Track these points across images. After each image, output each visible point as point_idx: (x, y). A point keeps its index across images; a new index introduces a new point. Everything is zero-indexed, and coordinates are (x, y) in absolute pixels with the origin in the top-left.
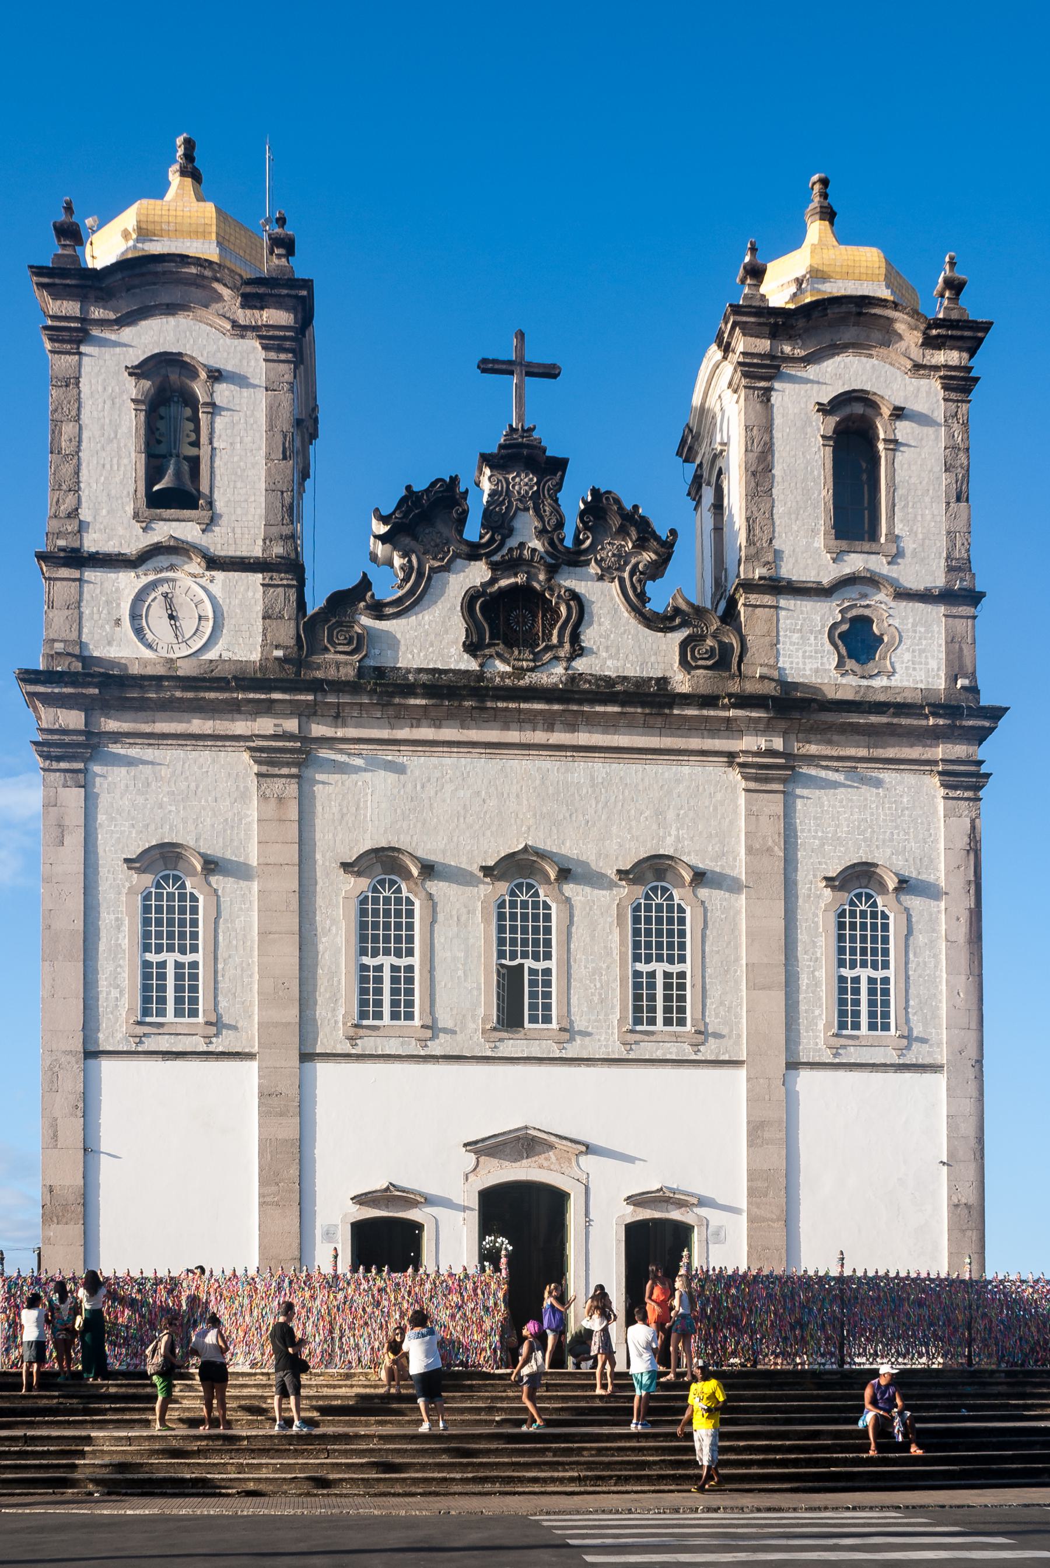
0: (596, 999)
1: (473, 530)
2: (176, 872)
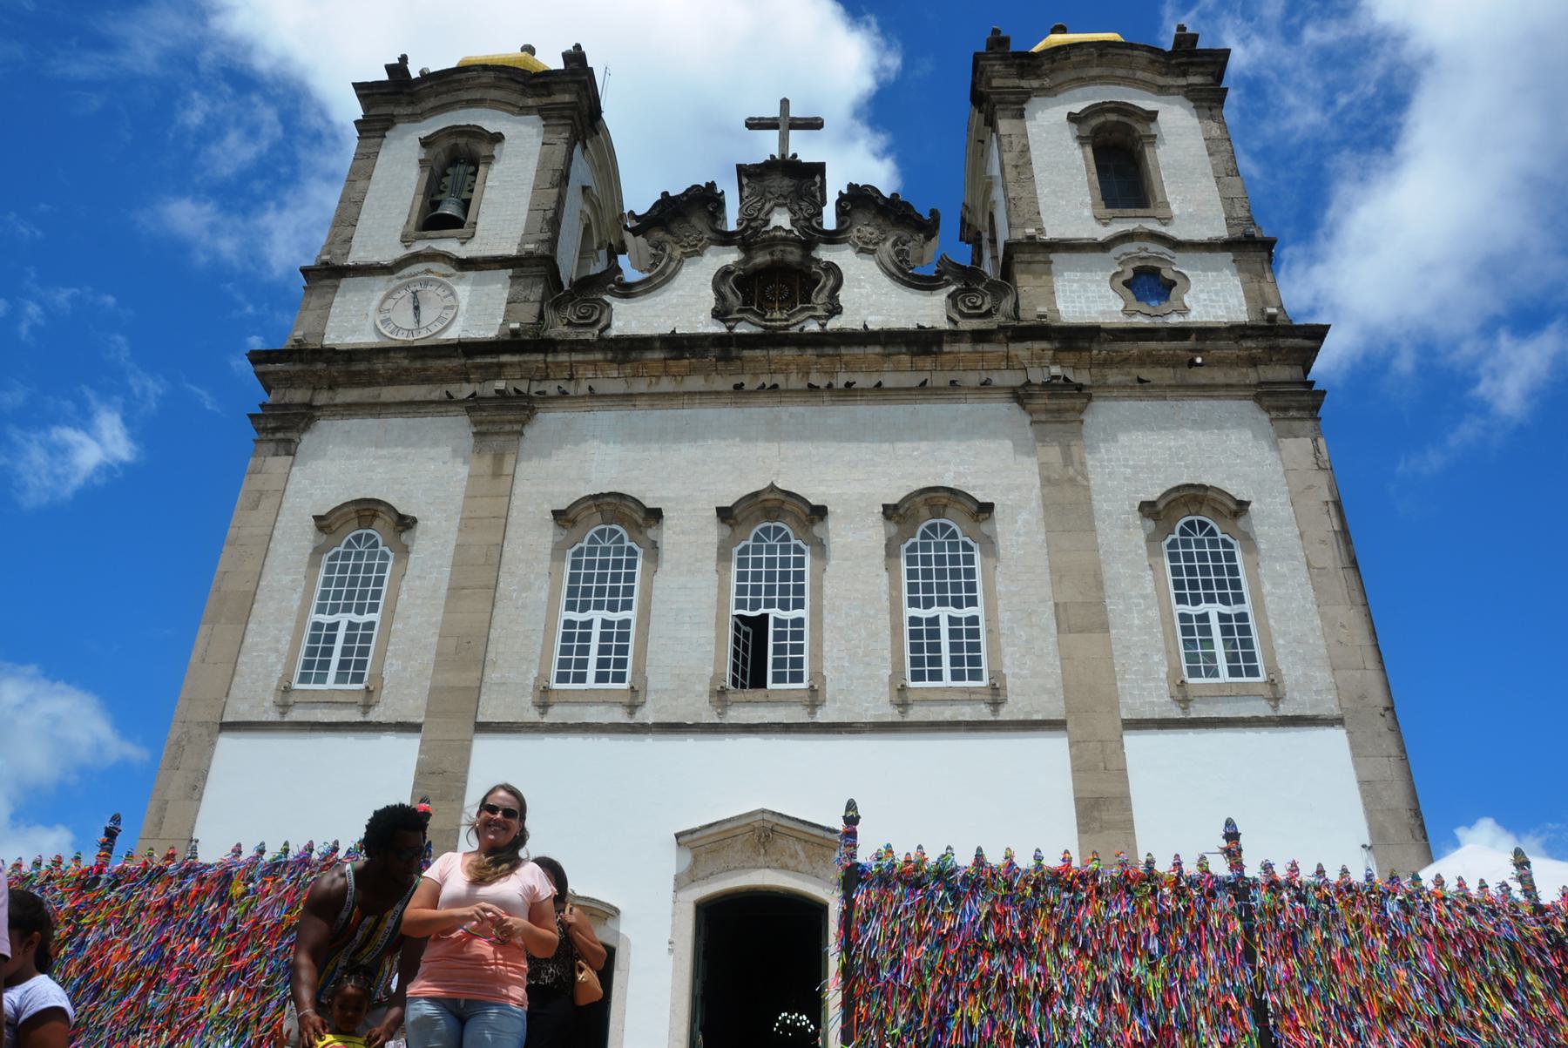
0: (860, 652)
1: (732, 225)
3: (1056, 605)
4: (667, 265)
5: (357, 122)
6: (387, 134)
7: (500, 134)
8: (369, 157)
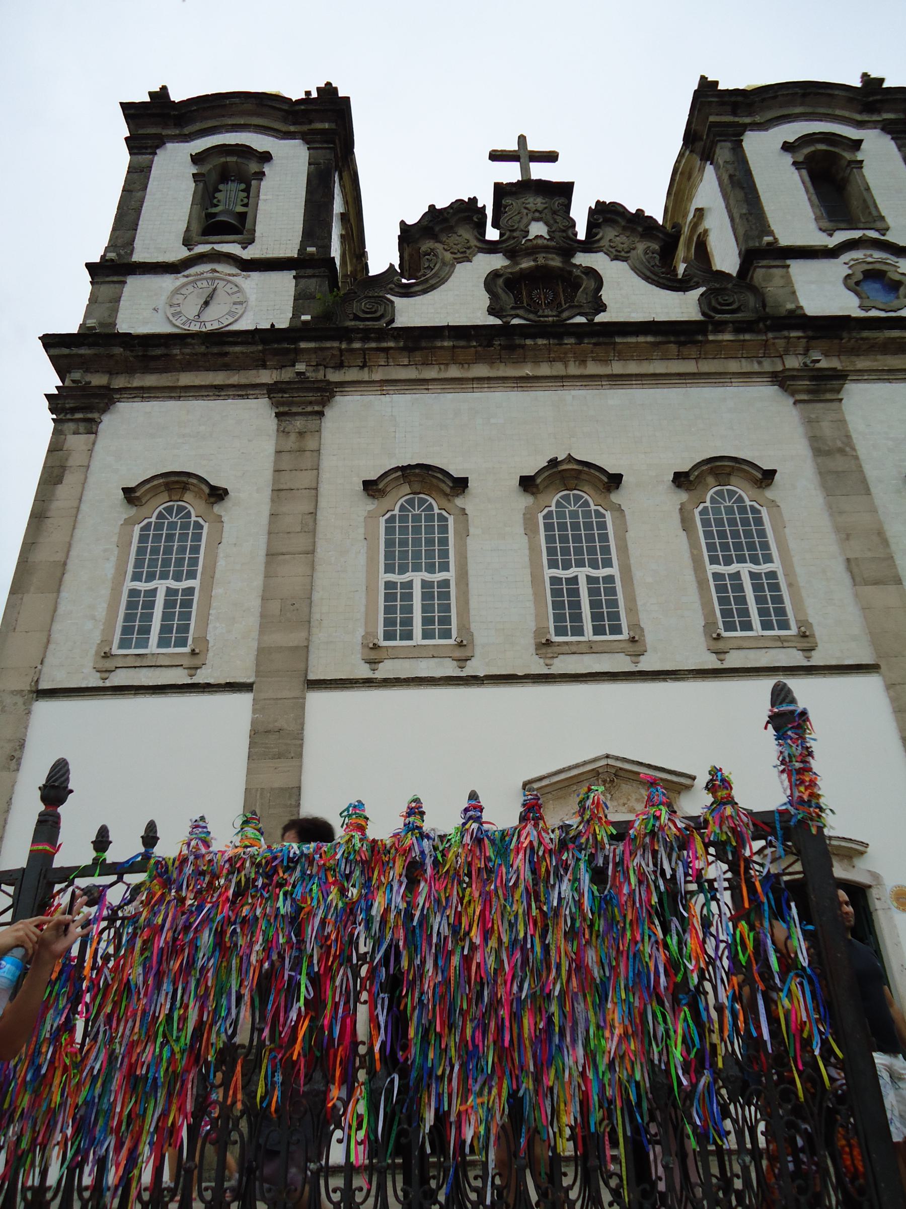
2: (180, 503)
3: (848, 560)
4: (440, 269)
5: (126, 139)
6: (158, 151)
7: (268, 153)
8: (142, 171)
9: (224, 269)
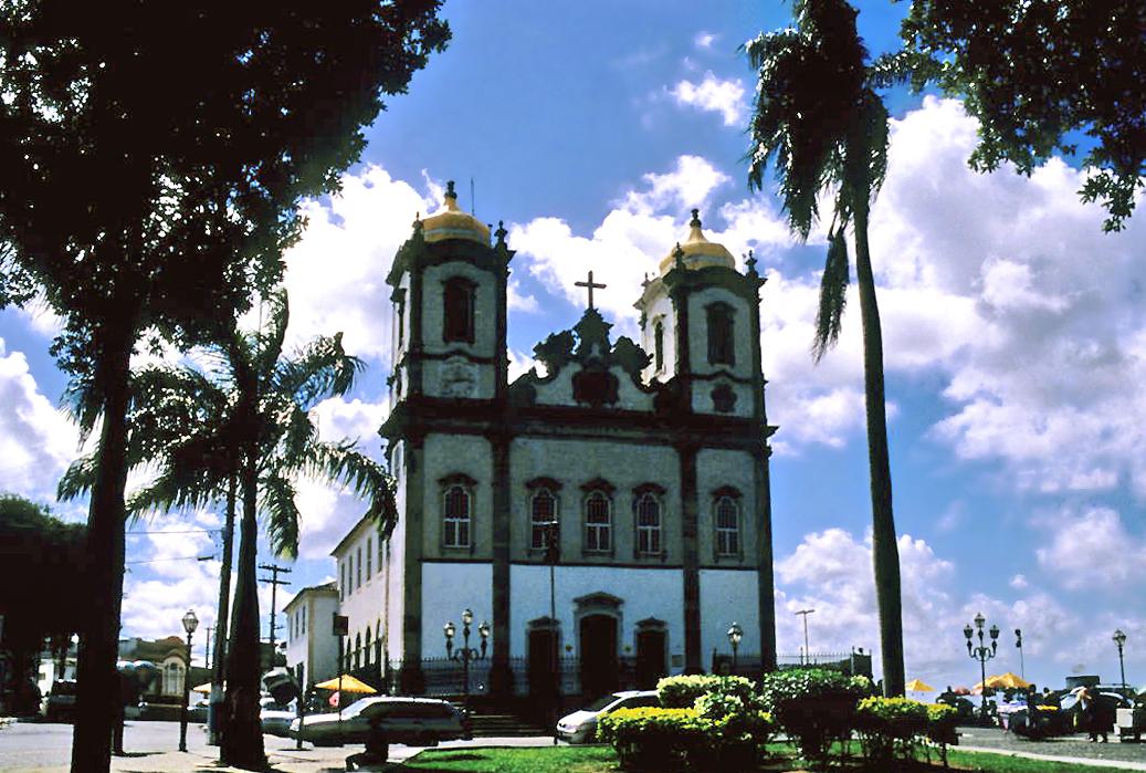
9: (464, 360)
